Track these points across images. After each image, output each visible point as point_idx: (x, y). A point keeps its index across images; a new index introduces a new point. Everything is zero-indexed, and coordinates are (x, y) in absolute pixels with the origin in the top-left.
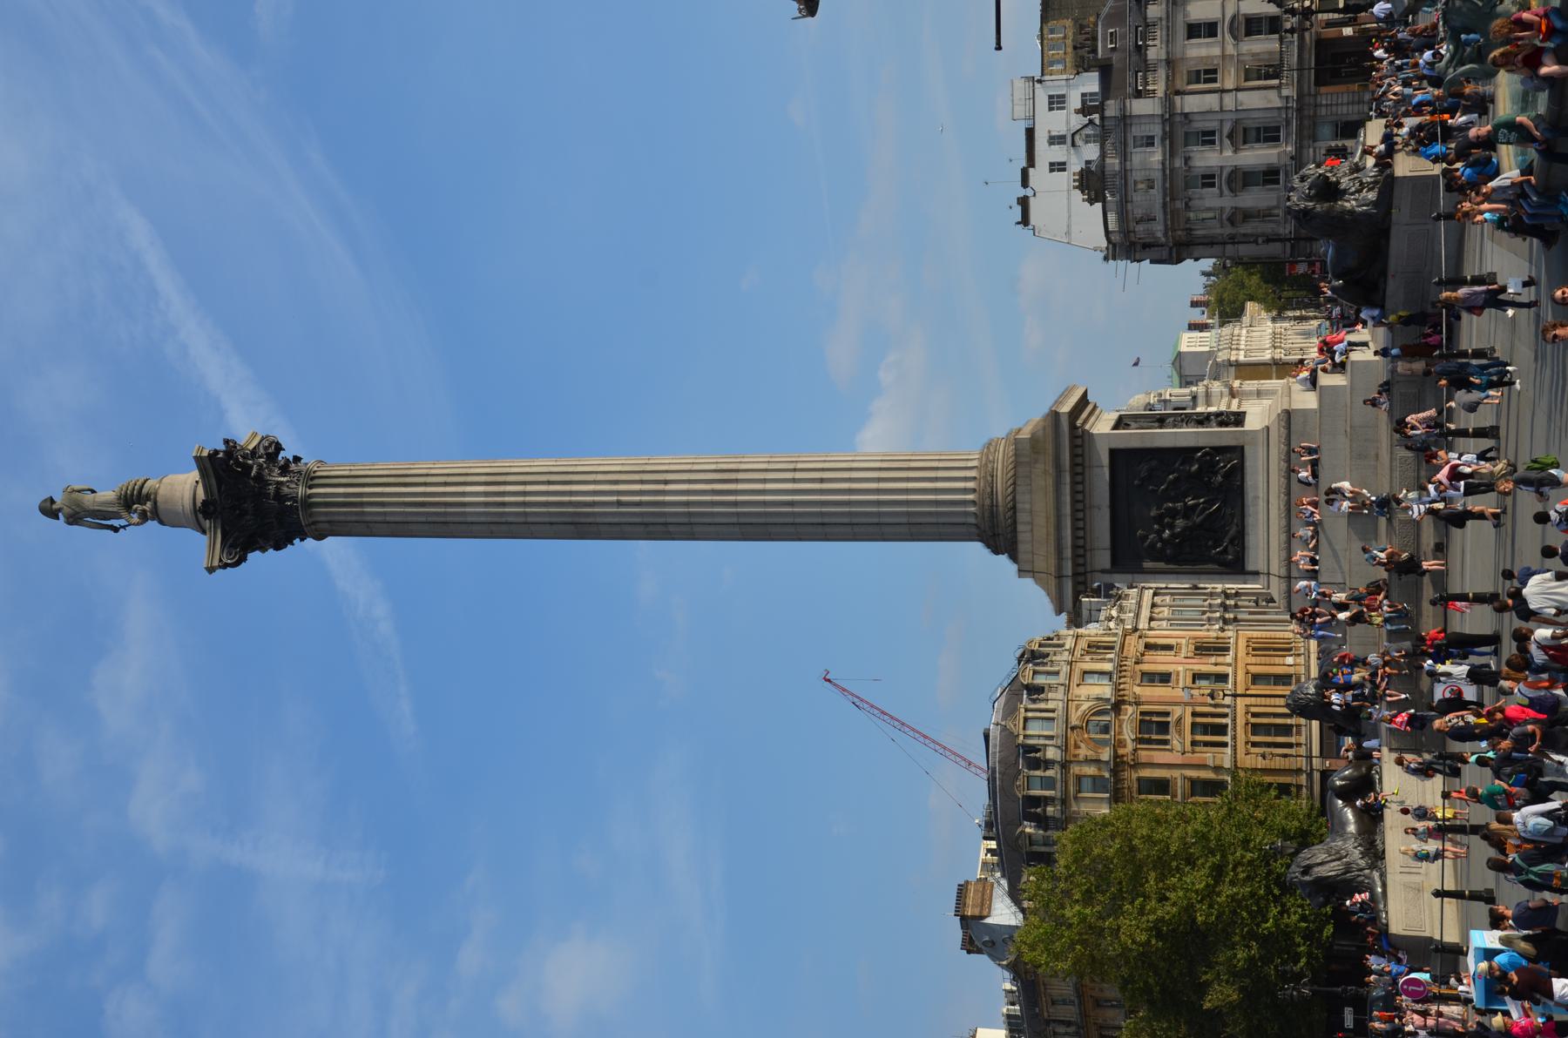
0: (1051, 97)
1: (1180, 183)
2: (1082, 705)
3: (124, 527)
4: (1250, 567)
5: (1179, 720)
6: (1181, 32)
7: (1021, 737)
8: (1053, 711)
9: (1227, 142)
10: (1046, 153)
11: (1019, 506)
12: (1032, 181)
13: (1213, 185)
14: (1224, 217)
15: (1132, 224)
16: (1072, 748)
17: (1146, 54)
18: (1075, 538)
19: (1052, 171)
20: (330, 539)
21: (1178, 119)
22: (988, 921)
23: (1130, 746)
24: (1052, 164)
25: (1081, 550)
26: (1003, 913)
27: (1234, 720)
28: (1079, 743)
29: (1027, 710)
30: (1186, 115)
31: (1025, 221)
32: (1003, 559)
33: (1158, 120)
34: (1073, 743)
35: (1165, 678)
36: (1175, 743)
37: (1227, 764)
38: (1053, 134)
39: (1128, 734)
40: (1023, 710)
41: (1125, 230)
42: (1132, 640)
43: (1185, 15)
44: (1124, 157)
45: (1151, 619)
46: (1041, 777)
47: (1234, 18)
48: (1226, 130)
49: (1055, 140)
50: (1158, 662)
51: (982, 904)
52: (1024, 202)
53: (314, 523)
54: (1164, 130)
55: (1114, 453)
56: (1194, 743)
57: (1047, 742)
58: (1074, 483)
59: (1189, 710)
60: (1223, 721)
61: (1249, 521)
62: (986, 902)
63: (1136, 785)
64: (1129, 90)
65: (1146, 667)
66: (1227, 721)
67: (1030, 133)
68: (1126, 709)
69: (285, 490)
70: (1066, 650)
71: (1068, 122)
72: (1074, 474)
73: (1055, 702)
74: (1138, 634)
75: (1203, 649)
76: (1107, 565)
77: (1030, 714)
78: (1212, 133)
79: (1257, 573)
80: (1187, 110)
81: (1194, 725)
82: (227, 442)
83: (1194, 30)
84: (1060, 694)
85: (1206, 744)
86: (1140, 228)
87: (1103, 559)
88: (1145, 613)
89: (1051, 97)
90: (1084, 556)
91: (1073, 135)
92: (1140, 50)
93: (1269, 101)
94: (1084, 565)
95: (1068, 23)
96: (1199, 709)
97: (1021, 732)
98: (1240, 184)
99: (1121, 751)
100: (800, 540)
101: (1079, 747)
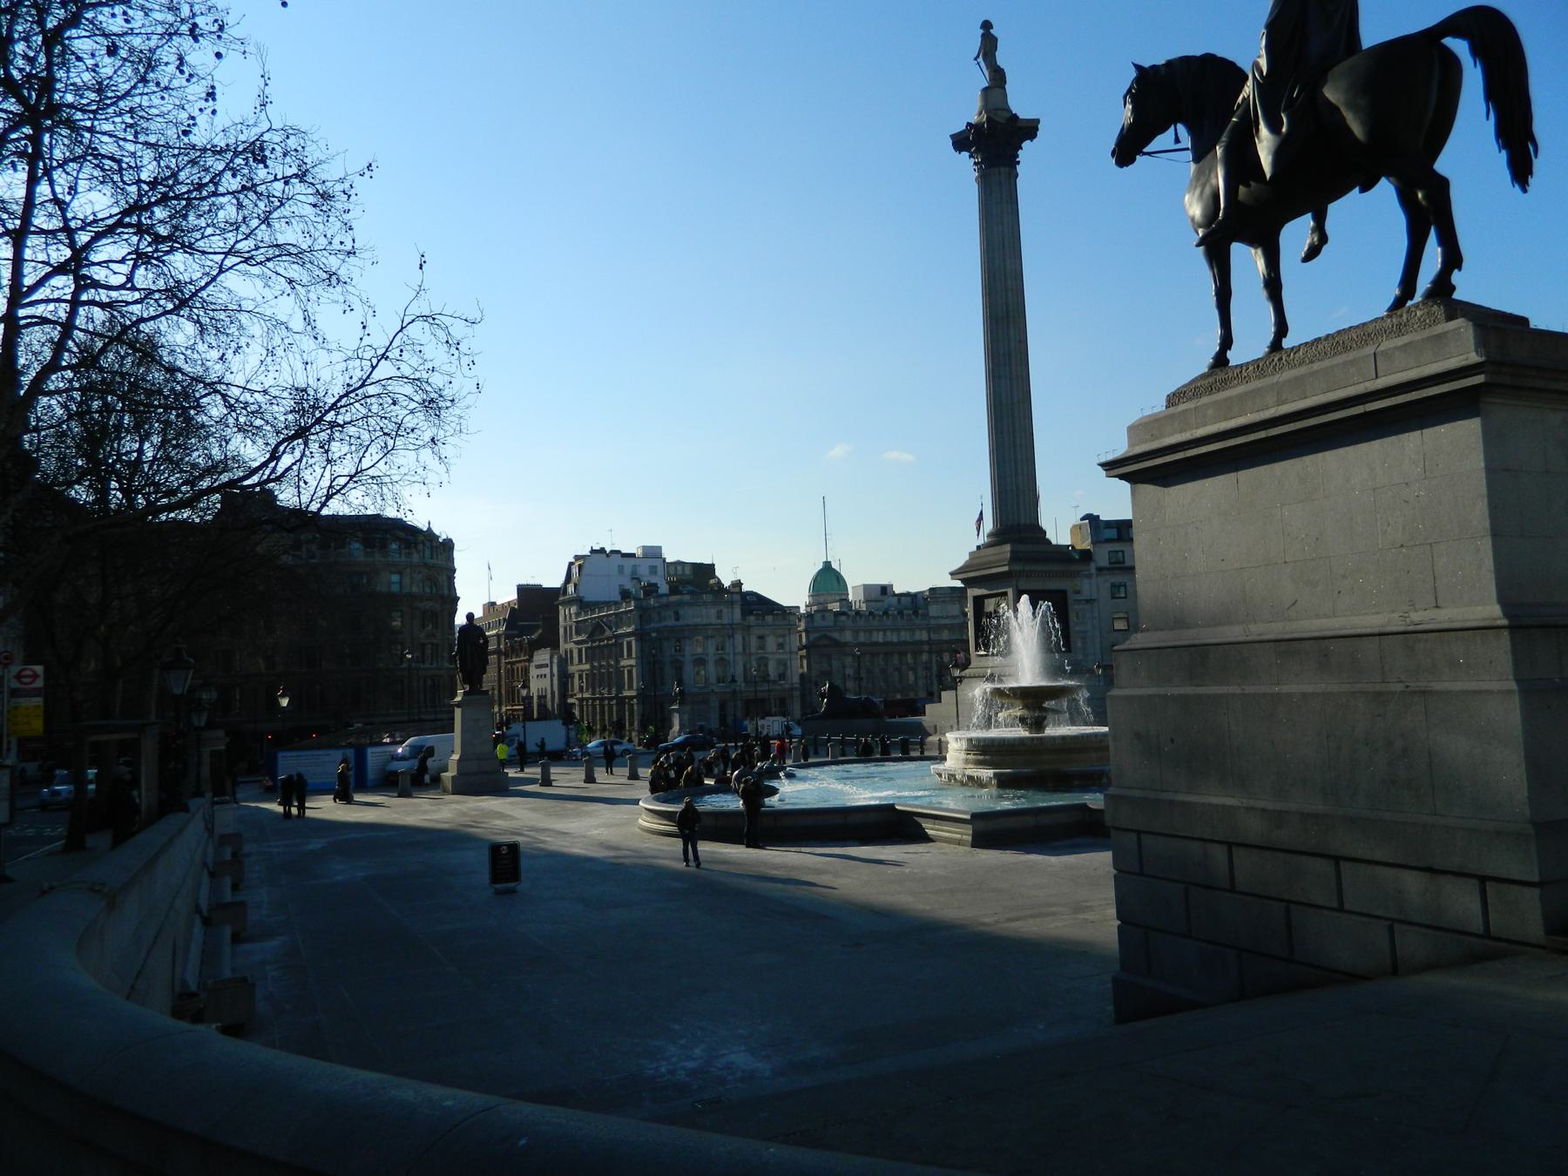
0: (656, 567)
3: (978, 63)
6: (760, 632)
19: (619, 566)
30: (733, 636)
31: (593, 551)
38: (638, 568)
39: (428, 605)
47: (767, 658)
48: (724, 656)
67: (633, 555)
80: (735, 636)
83: (761, 638)
86: (670, 613)
90: (1027, 576)
92: (751, 613)
95: (692, 577)
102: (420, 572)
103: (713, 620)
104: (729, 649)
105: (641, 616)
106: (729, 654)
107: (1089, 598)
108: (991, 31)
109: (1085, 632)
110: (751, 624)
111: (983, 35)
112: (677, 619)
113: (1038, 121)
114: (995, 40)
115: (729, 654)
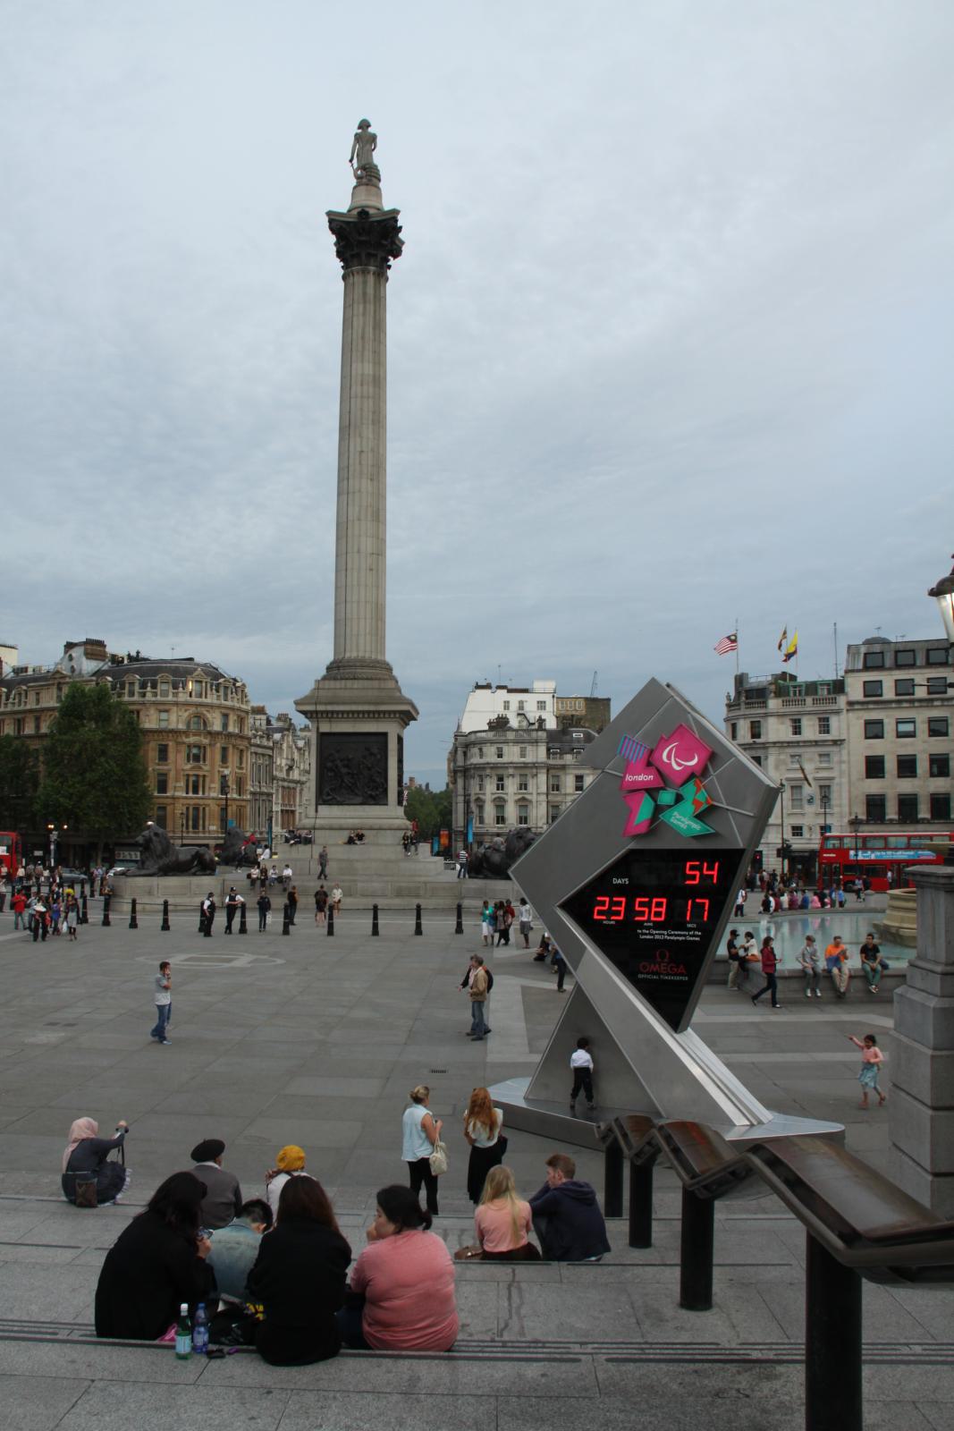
0: (545, 702)
1: (500, 772)
4: (320, 807)
5: (201, 768)
6: (579, 772)
9: (520, 796)
10: (514, 699)
11: (356, 681)
12: (498, 691)
13: (498, 789)
14: (481, 796)
15: (479, 746)
17: (569, 753)
18: (338, 712)
19: (505, 702)
20: (342, 284)
21: (534, 771)
22: (84, 659)
23: (187, 740)
24: (508, 702)
25: (331, 716)
26: (89, 666)
27: (202, 799)
30: (536, 775)
32: (324, 672)
33: (535, 761)
35: (224, 759)
36: (189, 766)
37: (178, 794)
39: (192, 740)
41: (474, 744)
42: (246, 743)
43: (588, 775)
44: (516, 742)
45: (256, 753)
49: (521, 705)
50: (233, 758)
51: (92, 654)
52: (488, 687)
53: (353, 275)
54: (528, 763)
55: (385, 735)
56: (188, 775)
58: (369, 712)
59: (206, 773)
60: (201, 793)
61: (346, 807)
63: (164, 743)
64: (550, 745)
65: (231, 750)
66: (200, 795)
69: (372, 261)
71: (531, 712)
72: (374, 712)
75: (240, 783)
76: (322, 730)
77: (204, 684)
78: (526, 789)
79: (317, 811)
80: (539, 775)
81: (197, 776)
82: (401, 227)
83: (579, 778)
84: (215, 701)
85: (188, 781)
87: (325, 728)
88: (260, 750)
89: (545, 702)
90: (327, 717)
91: (524, 714)
92: (571, 751)
93: (541, 819)
94: (322, 717)
96: (207, 780)
98: (498, 804)
100: (337, 556)
102: (186, 711)
103: (517, 759)
104: (531, 788)
105: (465, 754)
106: (532, 794)
107: (837, 738)
108: (370, 130)
109: (832, 779)
110: (568, 763)
111: (356, 135)
112: (481, 756)
113: (395, 212)
114: (373, 138)
115: (532, 794)
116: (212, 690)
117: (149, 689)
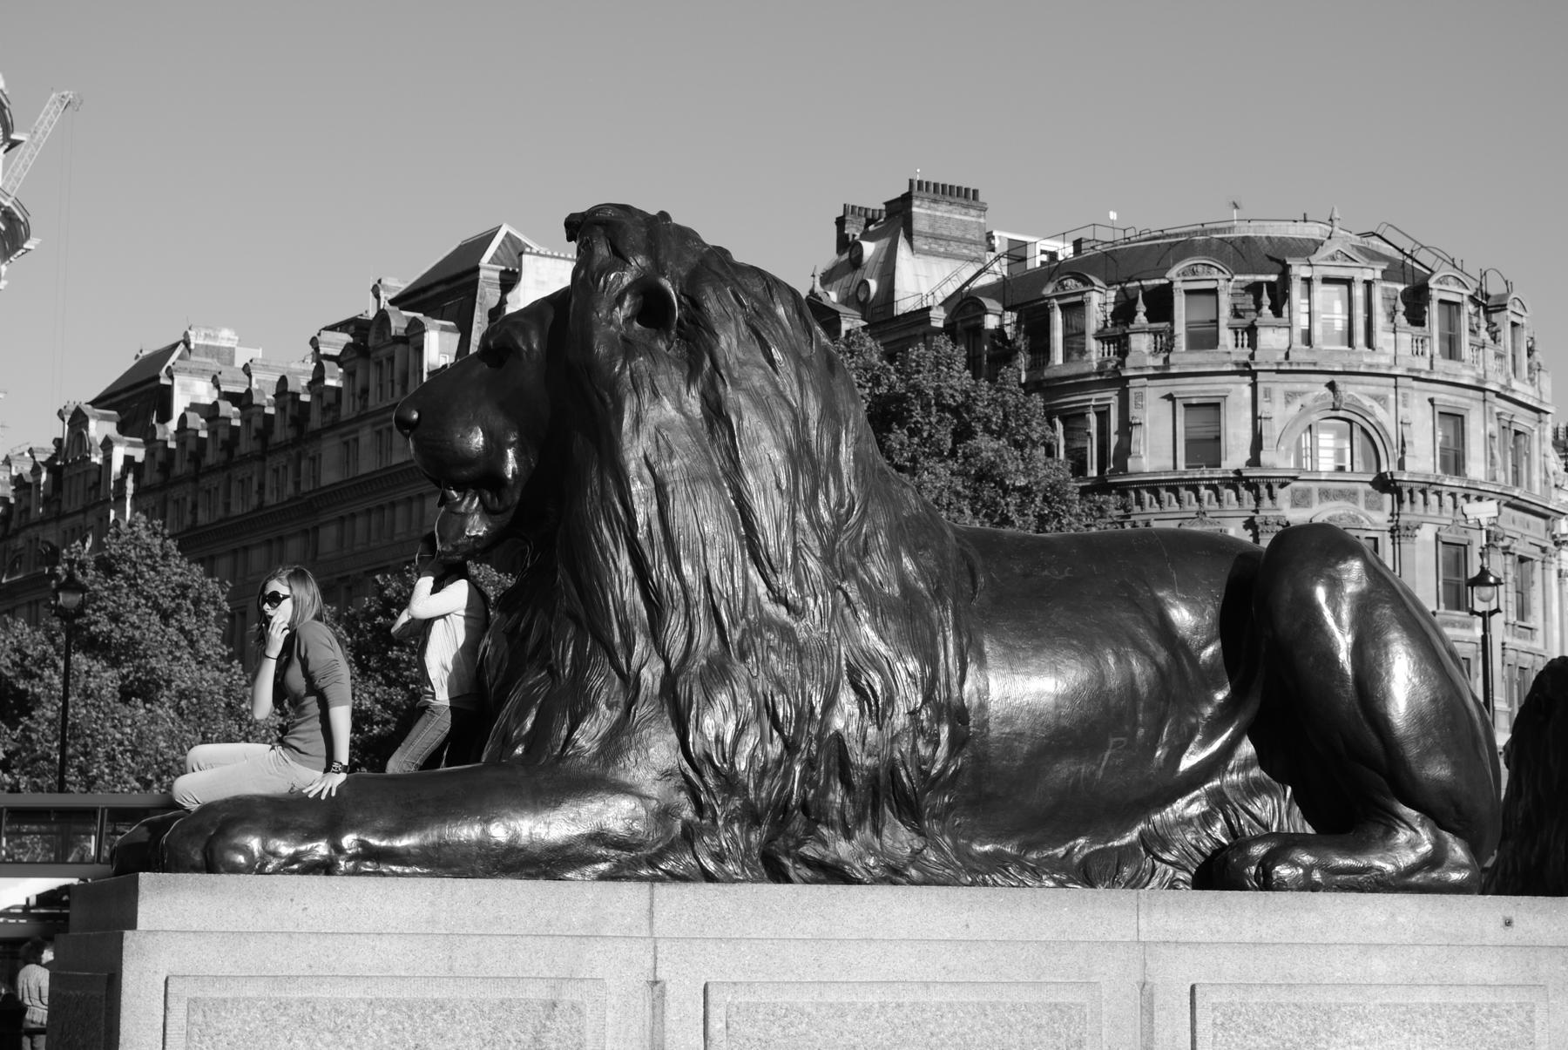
2: (1386, 409)
7: (1305, 272)
8: (1369, 343)
16: (1287, 387)
28: (1299, 402)
29: (1369, 284)
34: (1298, 387)
40: (1368, 275)
46: (1216, 321)
51: (936, 238)
57: (1297, 332)
62: (942, 245)
68: (1380, 509)
70: (1509, 381)
73: (1390, 349)
74: (1550, 545)
77: (1359, 292)
97: (1318, 273)
99: (1283, 494)
101: (1288, 402)
102: (1290, 397)
116: (1392, 316)
117: (1141, 318)
